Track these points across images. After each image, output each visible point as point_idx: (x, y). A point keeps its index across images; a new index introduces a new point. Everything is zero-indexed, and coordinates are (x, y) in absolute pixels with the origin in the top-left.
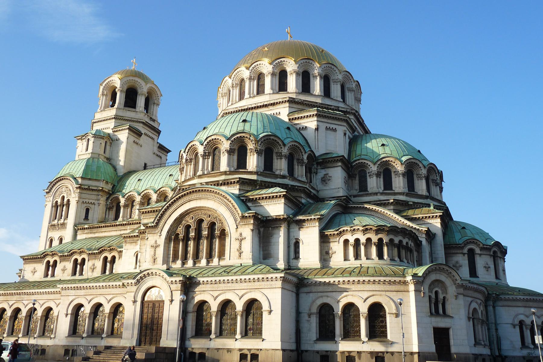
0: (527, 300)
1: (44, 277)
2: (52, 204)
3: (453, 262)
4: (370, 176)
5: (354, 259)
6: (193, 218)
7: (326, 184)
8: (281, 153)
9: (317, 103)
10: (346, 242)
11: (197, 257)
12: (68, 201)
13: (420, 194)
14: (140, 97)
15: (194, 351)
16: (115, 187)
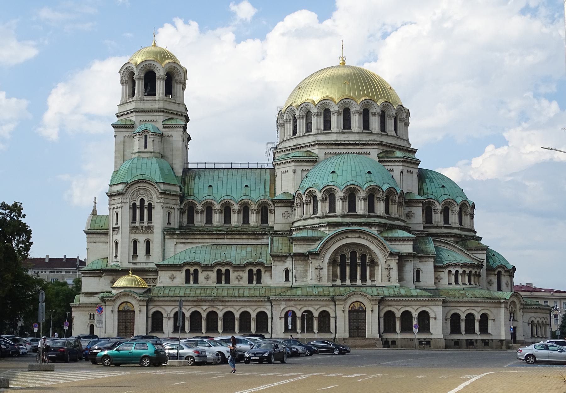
0: (536, 309)
1: (185, 283)
2: (130, 205)
3: (489, 280)
4: (435, 212)
5: (455, 283)
6: (347, 250)
7: (410, 219)
8: (395, 200)
9: (395, 145)
10: (450, 272)
11: (353, 278)
12: (150, 204)
13: (467, 227)
14: (178, 86)
15: (388, 340)
16: (183, 190)
